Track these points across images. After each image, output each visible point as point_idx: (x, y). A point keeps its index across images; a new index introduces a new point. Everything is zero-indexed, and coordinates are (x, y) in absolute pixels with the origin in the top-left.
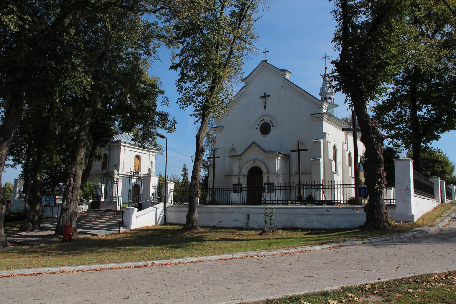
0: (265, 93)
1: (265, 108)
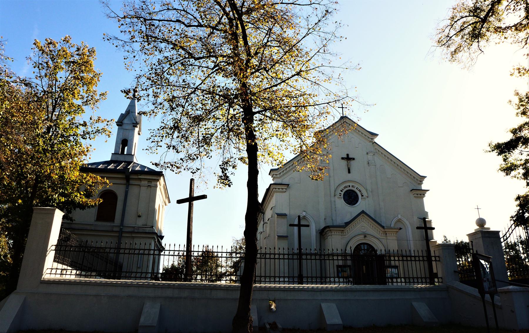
0: (348, 155)
1: (349, 172)
